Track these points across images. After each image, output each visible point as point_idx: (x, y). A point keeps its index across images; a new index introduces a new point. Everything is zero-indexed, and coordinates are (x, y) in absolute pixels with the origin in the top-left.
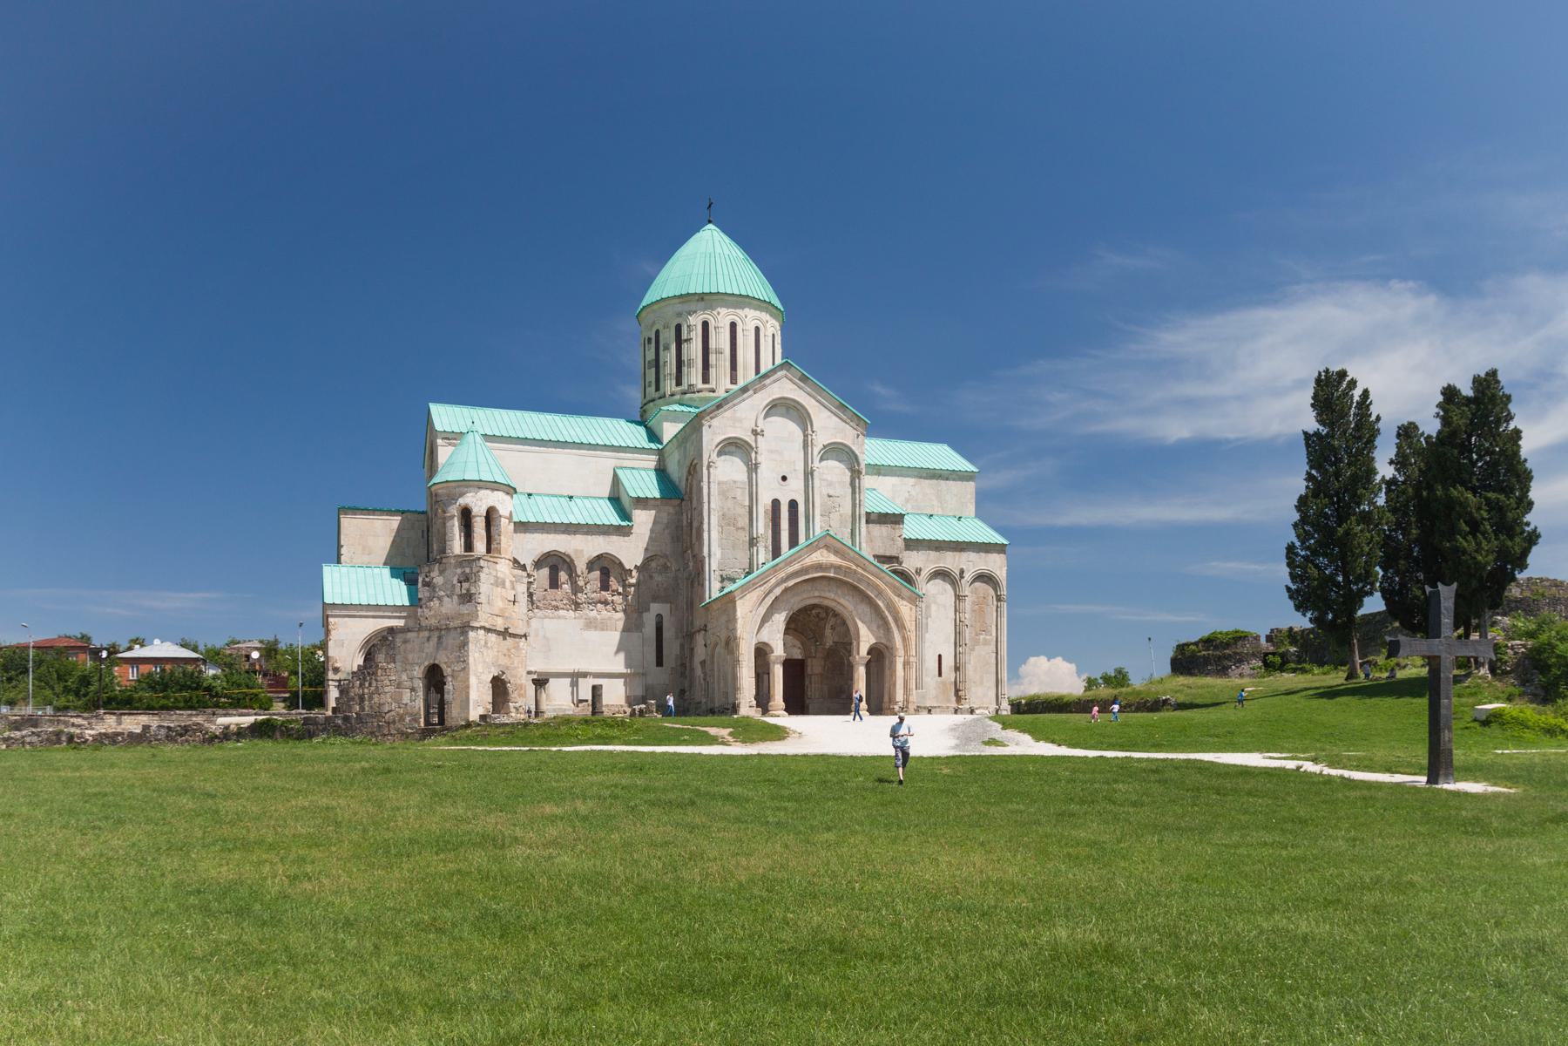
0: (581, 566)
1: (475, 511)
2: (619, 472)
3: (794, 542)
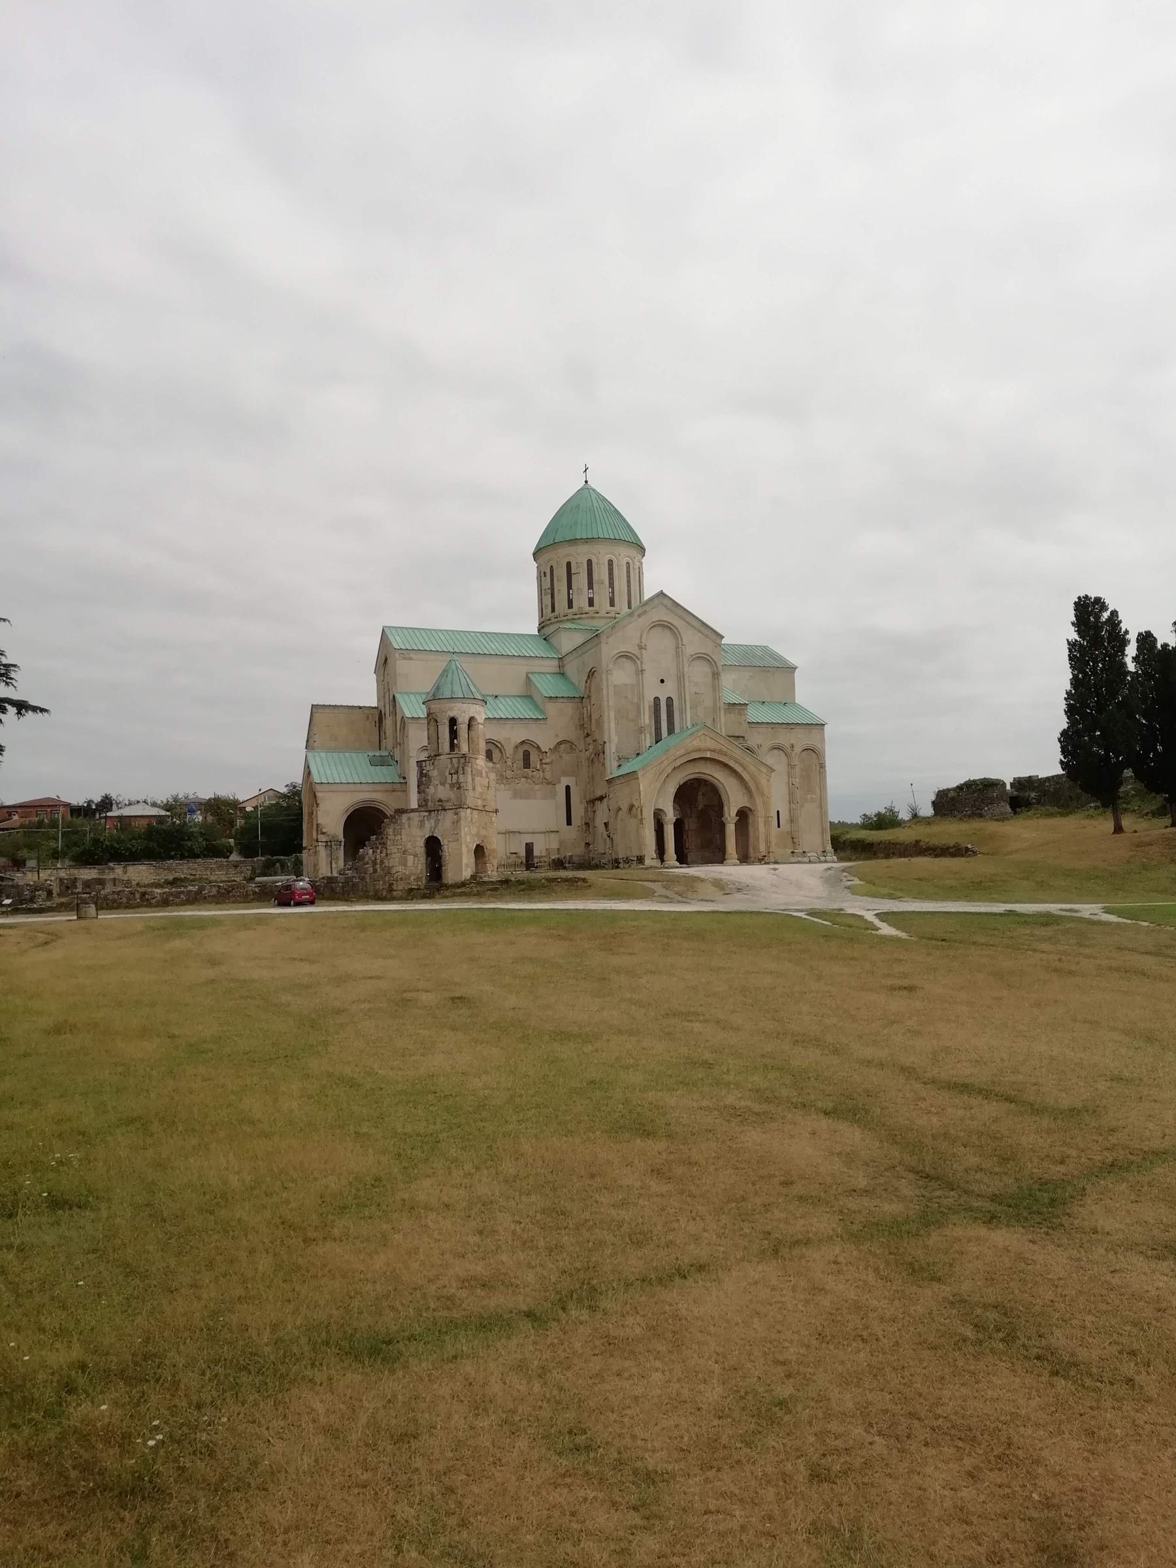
0: (509, 751)
1: (460, 720)
2: (530, 676)
3: (671, 730)
